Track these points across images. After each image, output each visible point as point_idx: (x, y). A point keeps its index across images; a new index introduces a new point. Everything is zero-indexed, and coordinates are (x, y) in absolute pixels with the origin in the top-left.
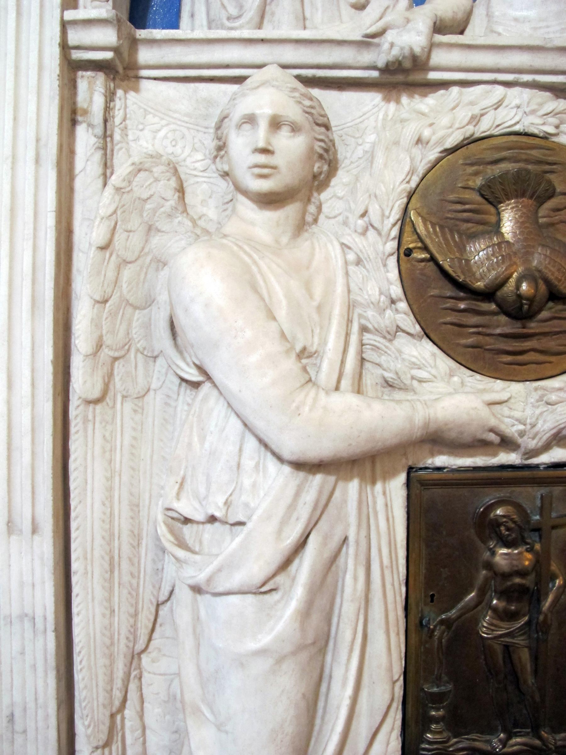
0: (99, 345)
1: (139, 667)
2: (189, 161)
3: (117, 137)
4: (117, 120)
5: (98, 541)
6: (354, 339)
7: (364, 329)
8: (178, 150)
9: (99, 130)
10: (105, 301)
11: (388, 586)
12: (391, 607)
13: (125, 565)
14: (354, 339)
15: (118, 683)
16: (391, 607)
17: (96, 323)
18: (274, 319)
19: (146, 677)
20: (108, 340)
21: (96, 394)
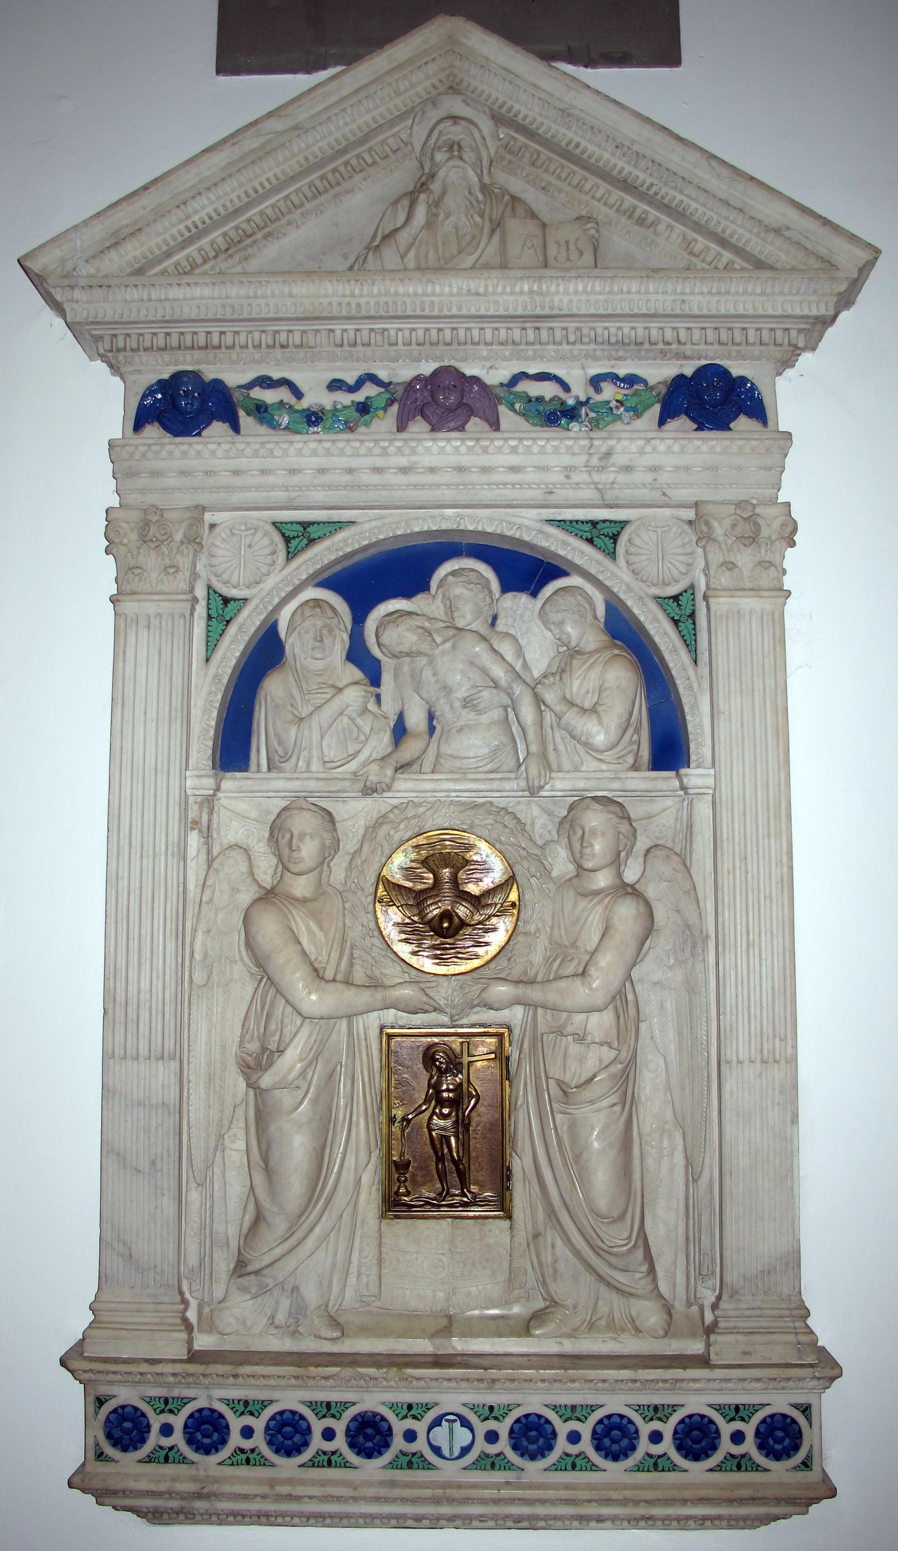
0: (206, 954)
1: (223, 1144)
2: (256, 848)
3: (215, 836)
4: (215, 826)
5: (203, 1064)
6: (347, 951)
7: (352, 947)
8: (250, 841)
9: (205, 835)
10: (209, 931)
11: (368, 1095)
12: (369, 1106)
13: (217, 1081)
14: (347, 951)
15: (211, 1150)
16: (369, 1106)
17: (204, 944)
18: (300, 943)
19: (227, 1152)
20: (210, 953)
21: (204, 982)
